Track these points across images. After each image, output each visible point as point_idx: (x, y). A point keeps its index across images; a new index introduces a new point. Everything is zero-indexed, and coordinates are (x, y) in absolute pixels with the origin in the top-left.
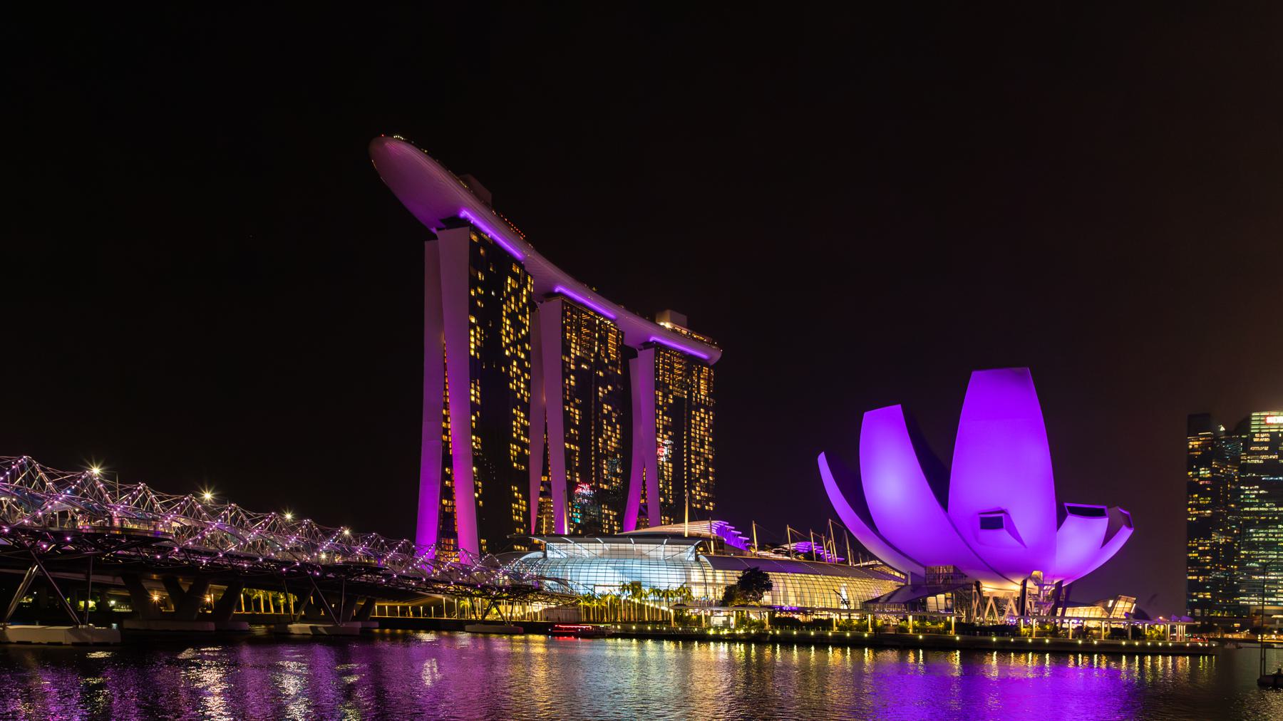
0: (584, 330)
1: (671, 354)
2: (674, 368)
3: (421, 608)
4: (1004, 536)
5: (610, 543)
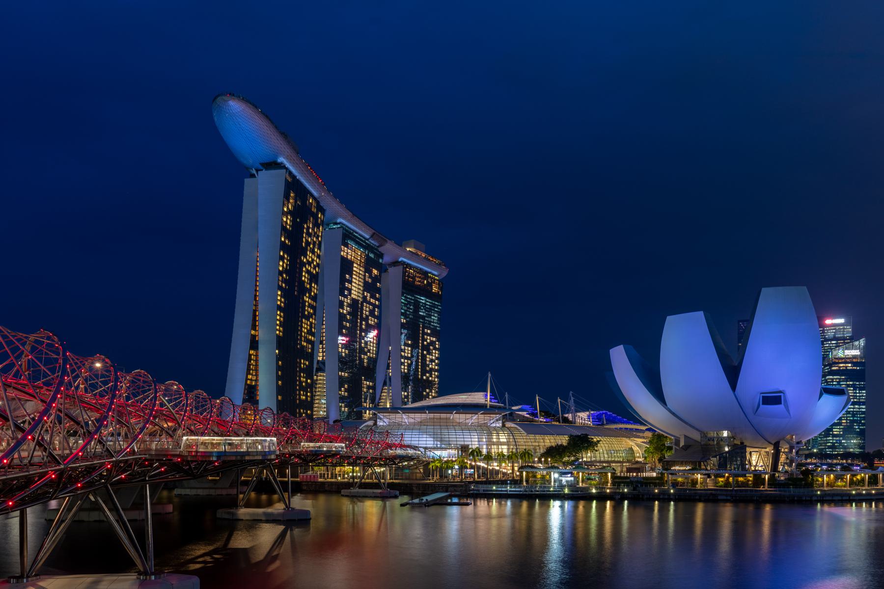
1: (414, 271)
2: (415, 280)
4: (780, 408)
5: (434, 413)
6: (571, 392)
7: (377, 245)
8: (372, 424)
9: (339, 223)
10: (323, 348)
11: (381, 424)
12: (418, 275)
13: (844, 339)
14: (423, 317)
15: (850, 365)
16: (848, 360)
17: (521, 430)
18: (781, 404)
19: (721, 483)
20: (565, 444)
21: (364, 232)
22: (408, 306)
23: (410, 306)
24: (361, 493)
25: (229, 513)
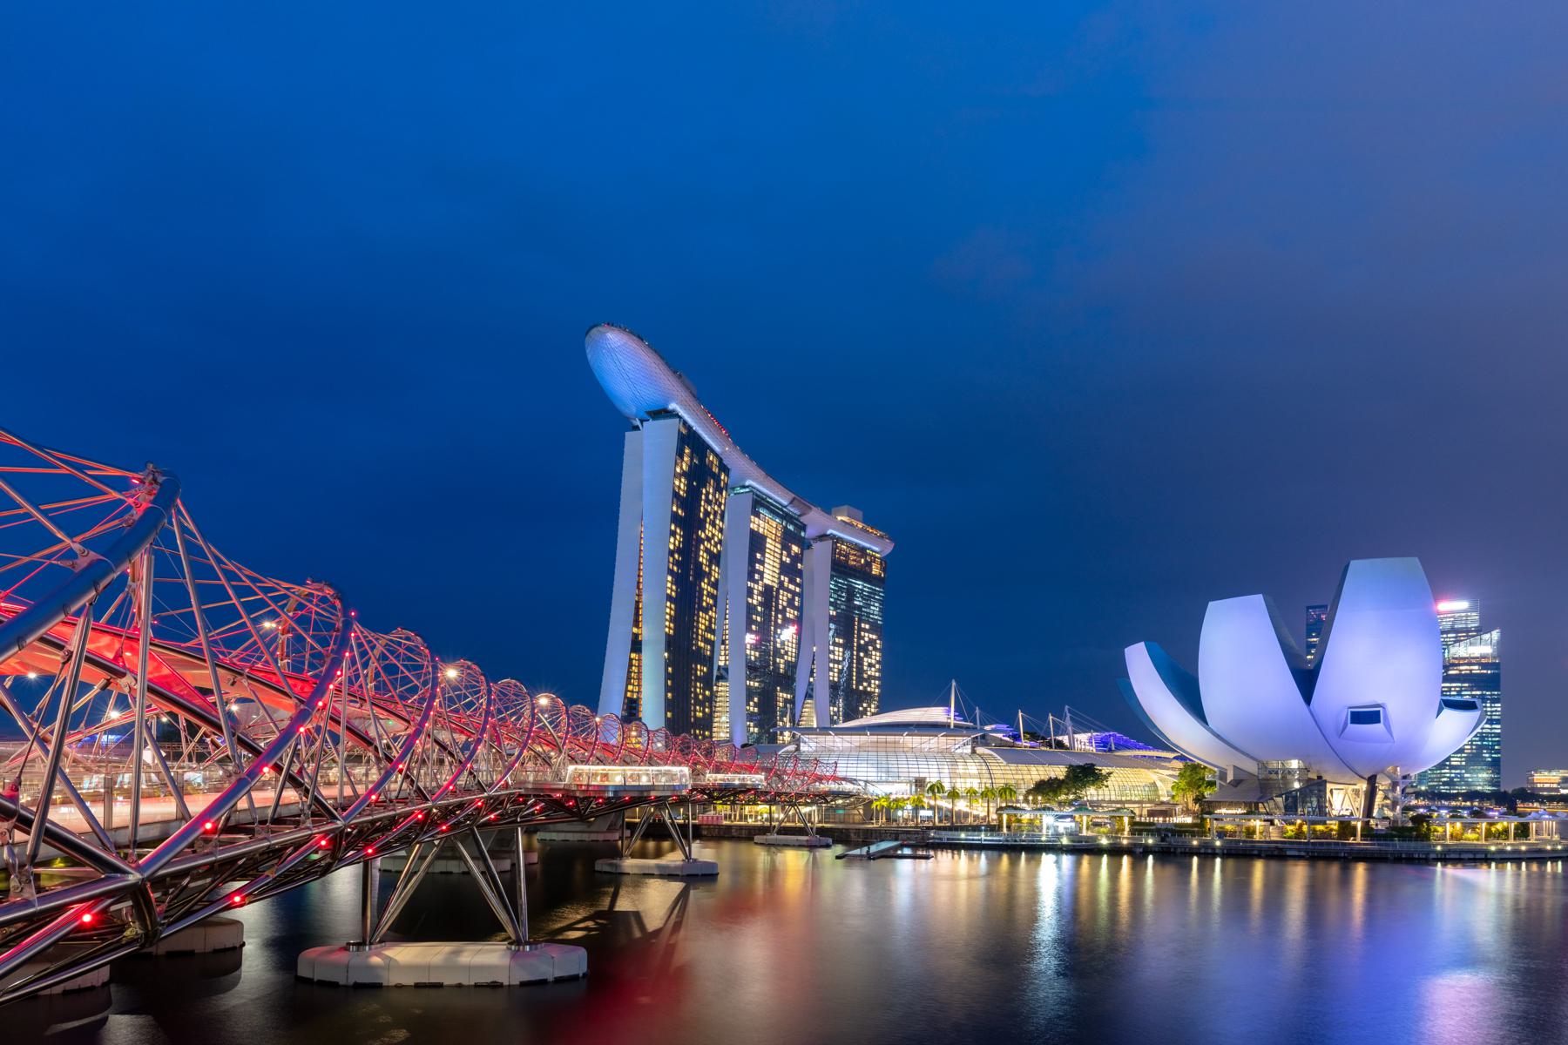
5: (878, 735)
6: (1067, 707)
7: (799, 513)
9: (748, 487)
10: (725, 650)
12: (852, 552)
13: (1467, 631)
14: (859, 608)
15: (1476, 667)
16: (1473, 661)
17: (999, 758)
18: (1379, 722)
19: (1290, 833)
20: (1061, 777)
21: (780, 497)
22: (839, 593)
23: (842, 592)
24: (781, 840)
25: (611, 865)
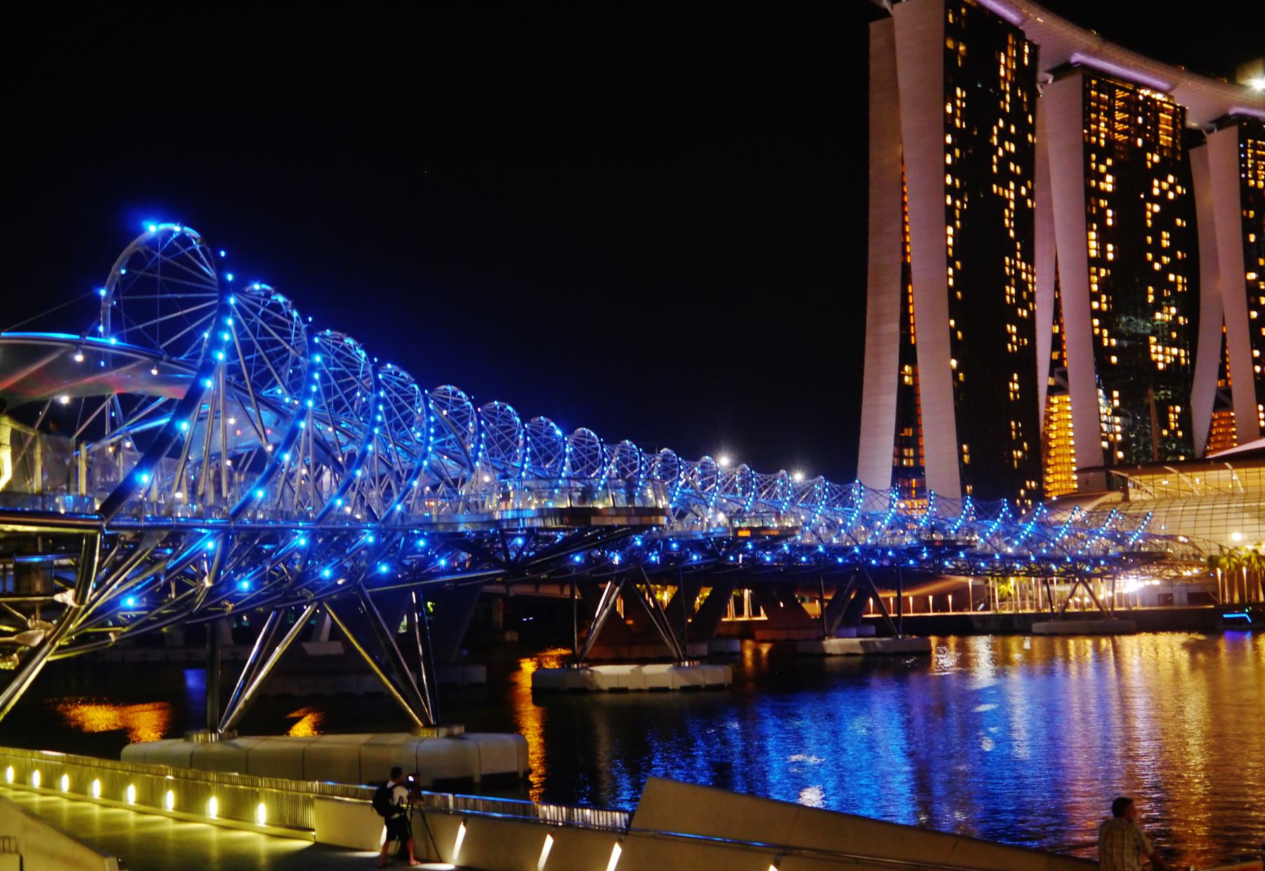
0: (1119, 116)
3: (931, 598)
8: (1120, 499)
11: (1138, 497)
